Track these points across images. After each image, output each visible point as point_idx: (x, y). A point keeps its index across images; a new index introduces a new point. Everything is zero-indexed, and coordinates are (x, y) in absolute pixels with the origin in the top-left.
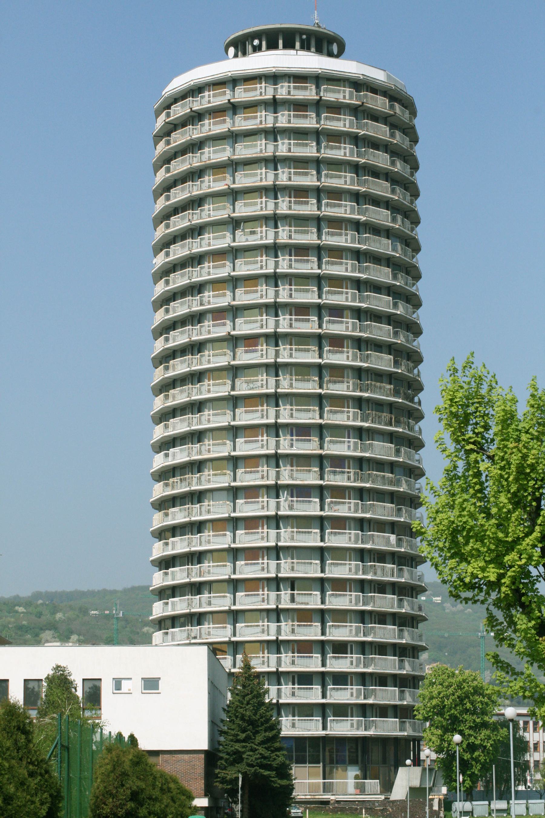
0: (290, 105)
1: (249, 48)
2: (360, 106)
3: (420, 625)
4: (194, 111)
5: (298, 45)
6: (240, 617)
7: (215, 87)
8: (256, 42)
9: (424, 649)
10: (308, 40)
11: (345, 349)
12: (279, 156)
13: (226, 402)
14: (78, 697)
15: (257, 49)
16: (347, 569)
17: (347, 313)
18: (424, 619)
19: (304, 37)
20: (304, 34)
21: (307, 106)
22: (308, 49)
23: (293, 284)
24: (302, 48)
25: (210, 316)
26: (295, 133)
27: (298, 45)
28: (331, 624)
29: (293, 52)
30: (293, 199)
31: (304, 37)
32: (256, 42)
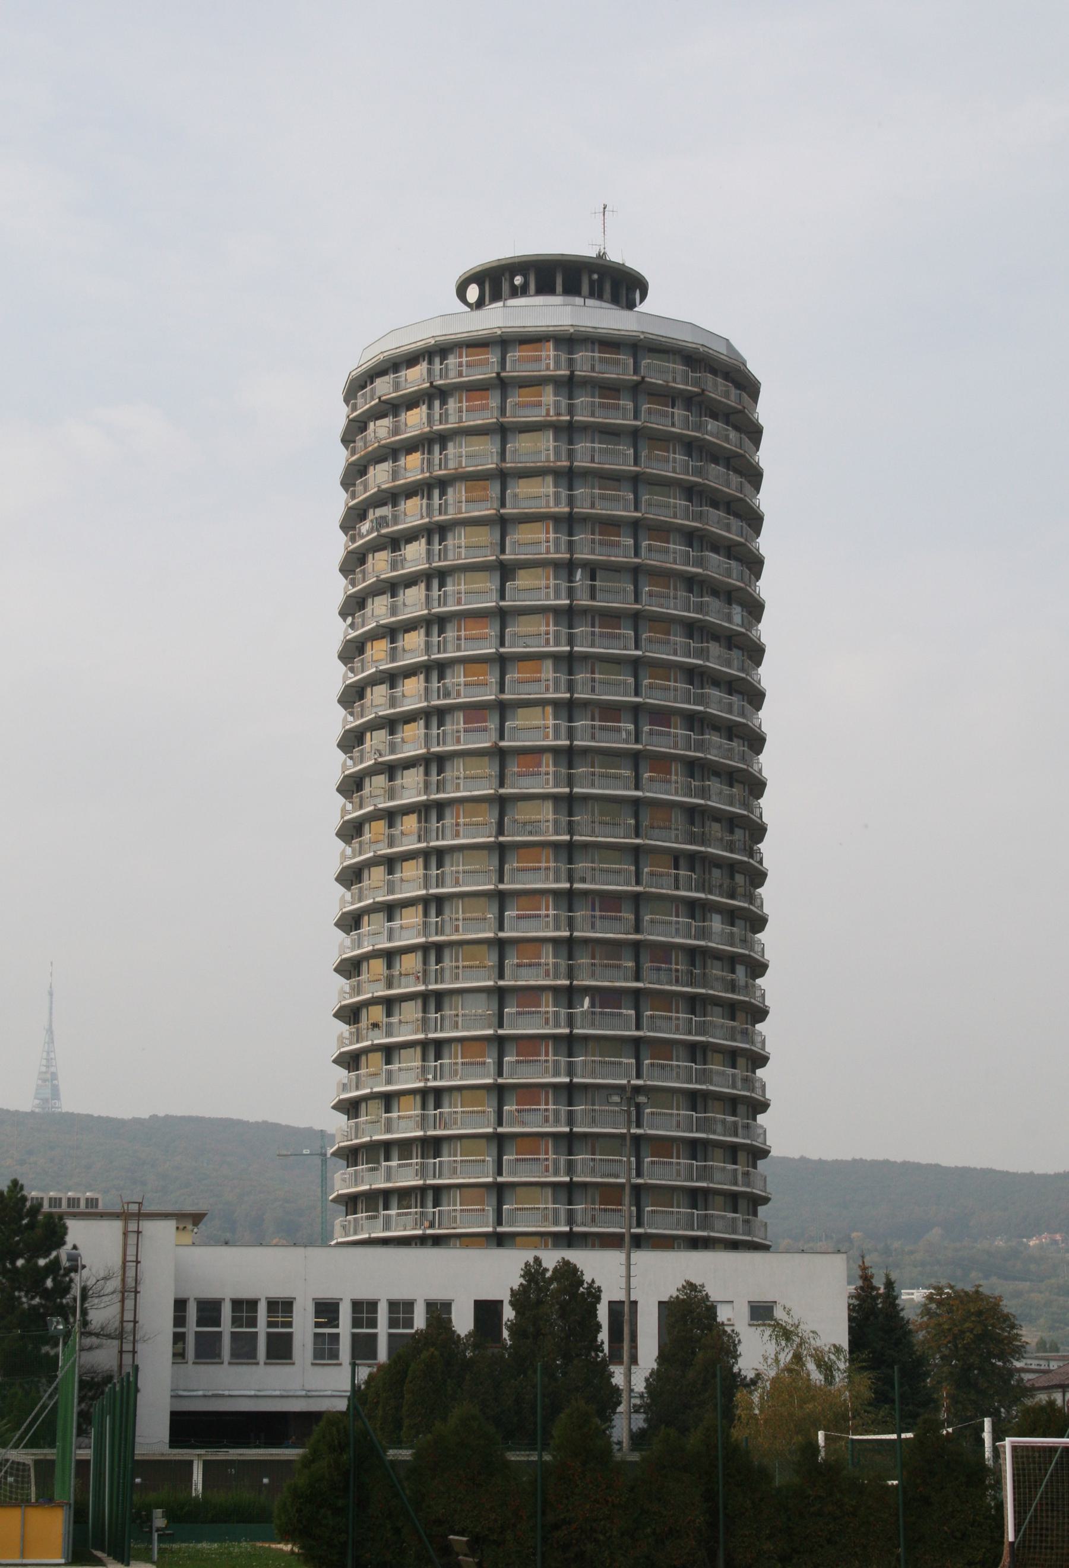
0: (593, 387)
1: (505, 288)
2: (698, 395)
3: (761, 1209)
4: (435, 387)
5: (585, 288)
6: (508, 1195)
7: (471, 350)
8: (518, 280)
9: (887, 1276)
10: (601, 281)
11: (674, 778)
12: (579, 467)
13: (486, 852)
14: (609, 1398)
15: (517, 292)
16: (674, 1123)
17: (677, 720)
18: (765, 1200)
19: (595, 276)
20: (595, 272)
21: (618, 390)
22: (600, 297)
23: (596, 671)
24: (592, 295)
25: (460, 716)
26: (601, 432)
27: (585, 288)
28: (649, 1209)
29: (578, 300)
30: (597, 537)
31: (595, 276)
32: (518, 280)
